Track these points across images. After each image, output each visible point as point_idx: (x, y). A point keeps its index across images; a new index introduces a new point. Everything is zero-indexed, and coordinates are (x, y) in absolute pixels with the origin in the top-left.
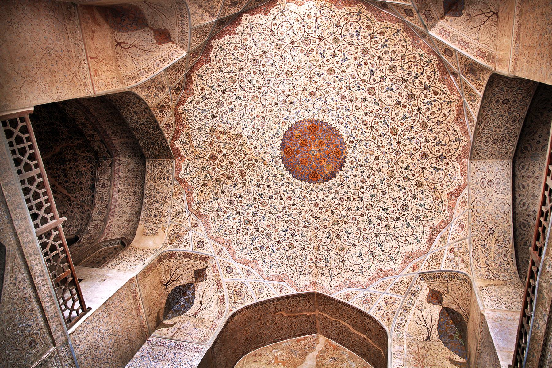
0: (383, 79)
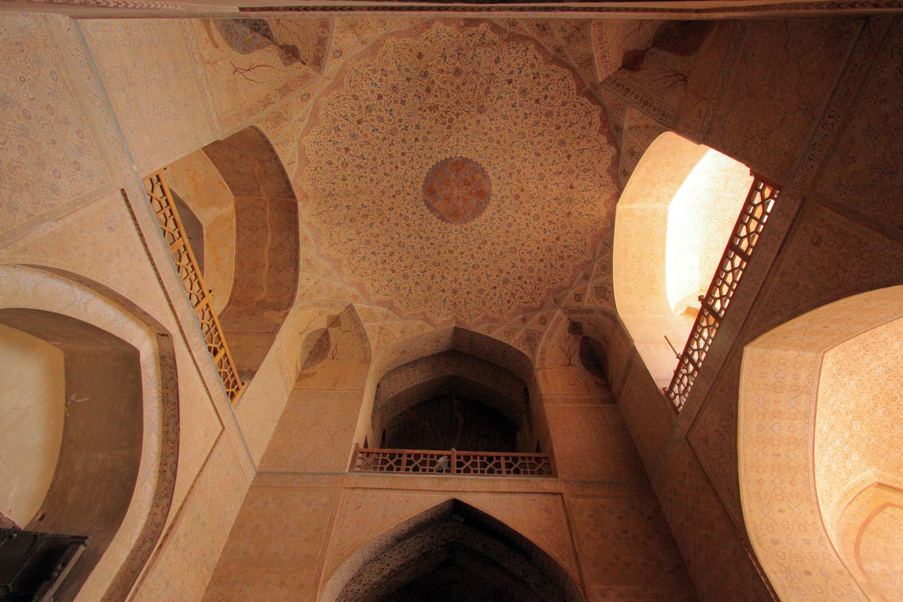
0: (523, 260)
